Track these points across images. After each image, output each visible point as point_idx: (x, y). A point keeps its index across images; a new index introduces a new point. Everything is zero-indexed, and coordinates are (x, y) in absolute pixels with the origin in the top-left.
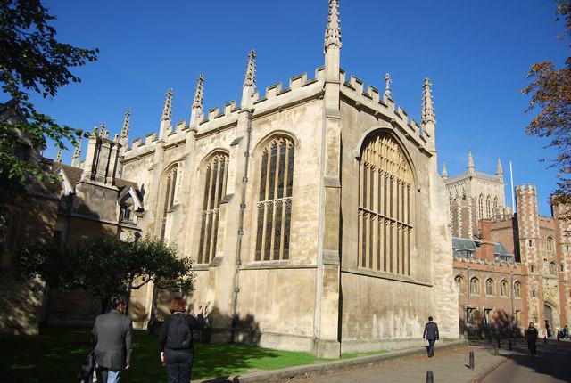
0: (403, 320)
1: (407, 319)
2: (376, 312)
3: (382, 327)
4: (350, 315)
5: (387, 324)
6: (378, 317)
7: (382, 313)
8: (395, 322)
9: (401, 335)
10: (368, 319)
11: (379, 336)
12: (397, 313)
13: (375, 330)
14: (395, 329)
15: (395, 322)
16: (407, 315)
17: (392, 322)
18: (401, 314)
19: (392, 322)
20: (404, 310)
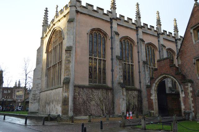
0: (55, 106)
1: (56, 105)
2: (47, 104)
3: (48, 109)
4: (43, 106)
5: (50, 108)
6: (48, 105)
7: (49, 104)
8: (52, 107)
9: (54, 112)
10: (45, 106)
11: (47, 113)
12: (53, 103)
13: (47, 110)
14: (52, 110)
15: (52, 107)
16: (56, 103)
17: (51, 107)
18: (54, 103)
19: (51, 107)
20: (55, 102)
